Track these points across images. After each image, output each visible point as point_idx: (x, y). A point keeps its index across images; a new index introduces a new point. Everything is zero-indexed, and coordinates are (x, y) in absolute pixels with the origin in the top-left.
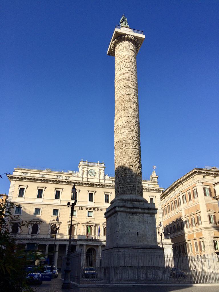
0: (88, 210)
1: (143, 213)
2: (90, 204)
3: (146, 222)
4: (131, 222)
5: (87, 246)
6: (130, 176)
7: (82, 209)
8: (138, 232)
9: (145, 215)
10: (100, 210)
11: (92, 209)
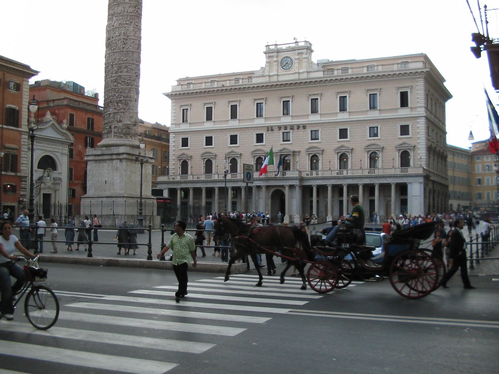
0: (283, 130)
1: (112, 159)
2: (286, 120)
3: (115, 169)
4: (100, 171)
5: (268, 187)
6: (108, 115)
7: (272, 130)
8: (106, 181)
9: (115, 162)
10: (301, 128)
11: (289, 128)
